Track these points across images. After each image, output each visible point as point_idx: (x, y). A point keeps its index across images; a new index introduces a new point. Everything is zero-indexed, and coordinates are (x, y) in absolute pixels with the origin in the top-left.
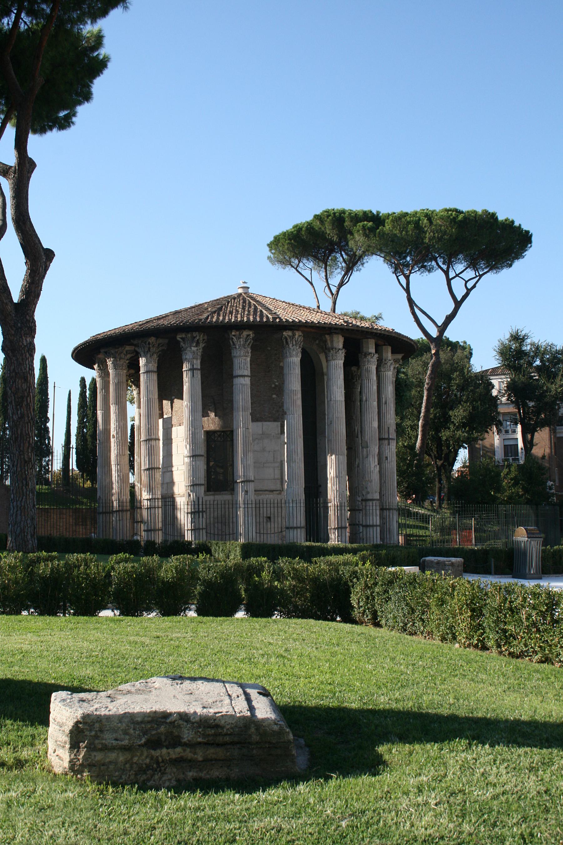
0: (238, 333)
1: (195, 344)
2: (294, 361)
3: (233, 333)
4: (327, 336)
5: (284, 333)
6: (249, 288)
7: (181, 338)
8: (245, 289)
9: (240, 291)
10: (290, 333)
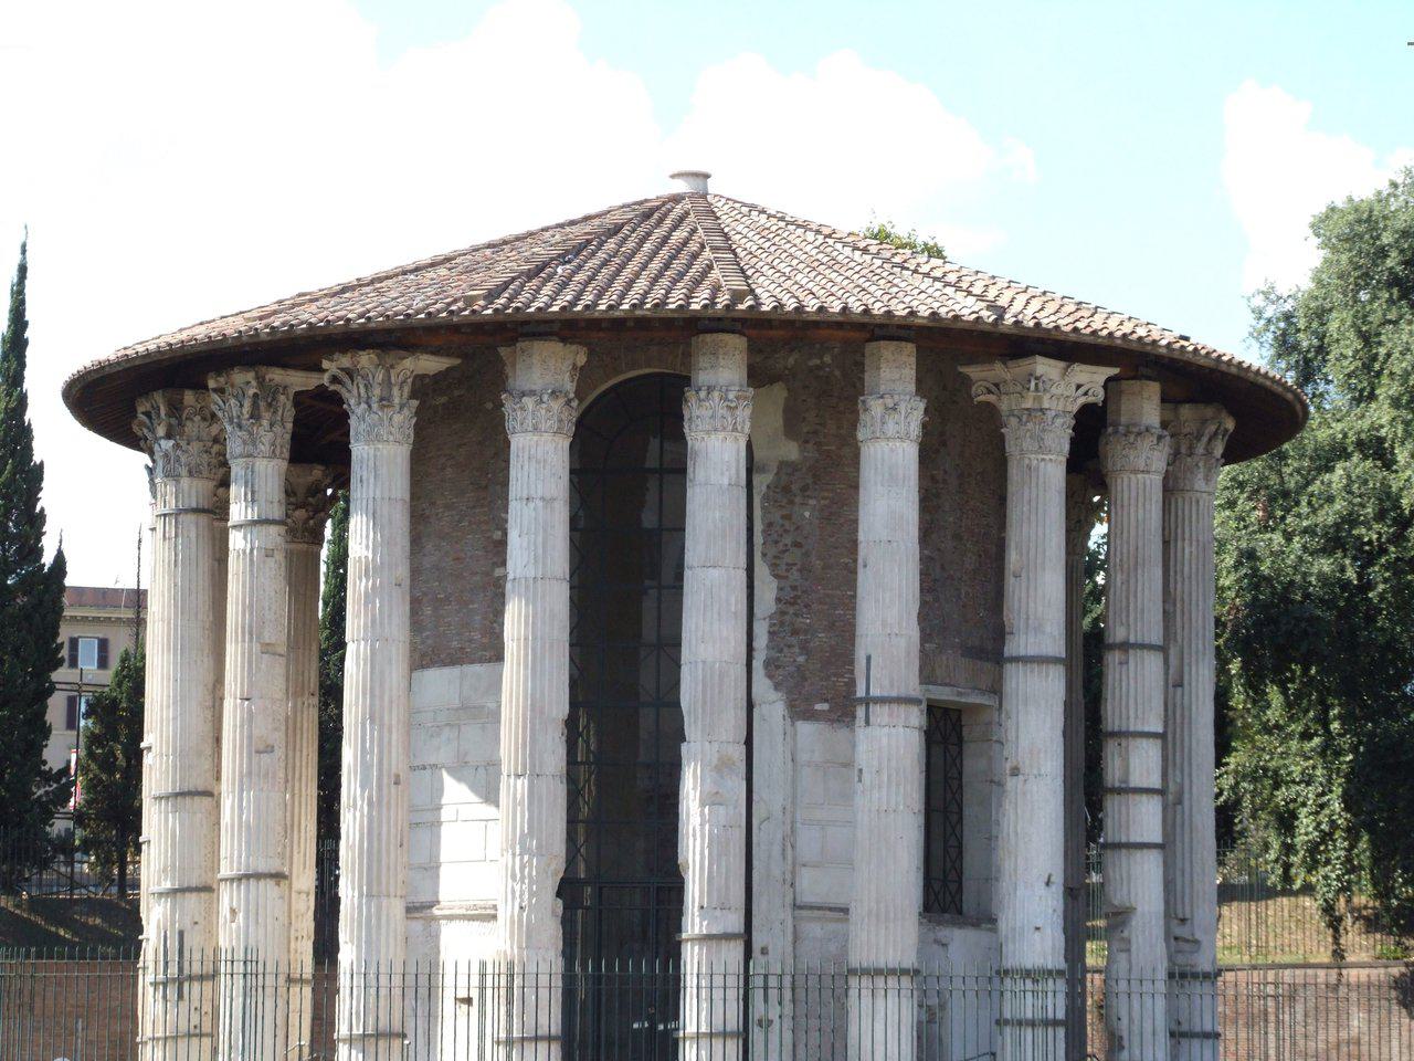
0: (222, 380)
1: (161, 431)
2: (380, 455)
3: (212, 384)
4: (503, 351)
5: (325, 364)
6: (707, 176)
7: (148, 414)
8: (700, 181)
9: (681, 187)
10: (345, 361)
